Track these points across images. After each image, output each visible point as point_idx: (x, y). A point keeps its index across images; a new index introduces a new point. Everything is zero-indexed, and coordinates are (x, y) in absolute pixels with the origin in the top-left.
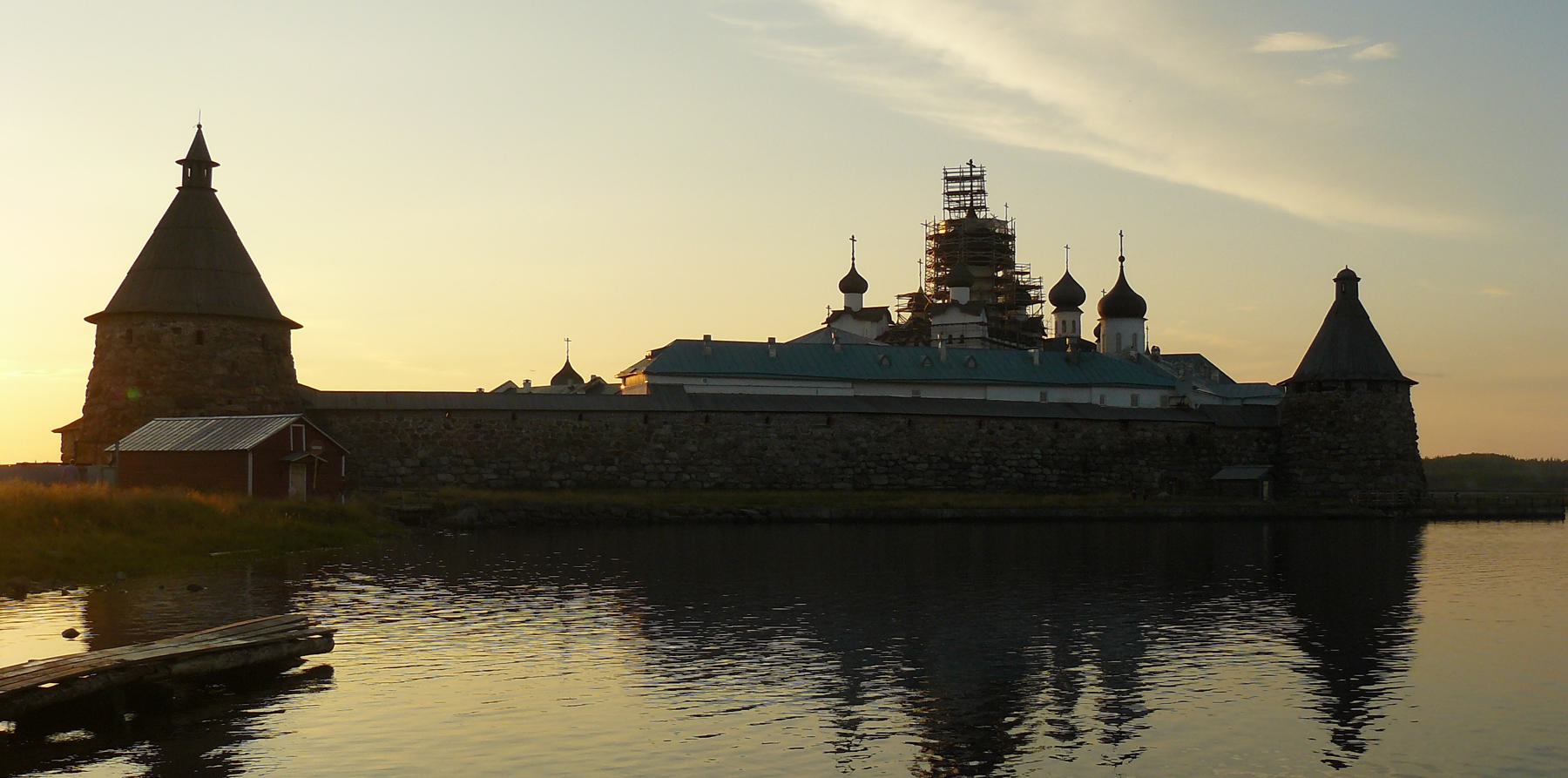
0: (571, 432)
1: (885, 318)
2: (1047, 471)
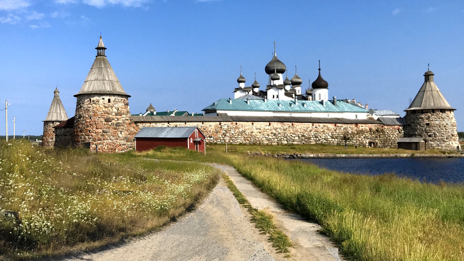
0: (201, 128)
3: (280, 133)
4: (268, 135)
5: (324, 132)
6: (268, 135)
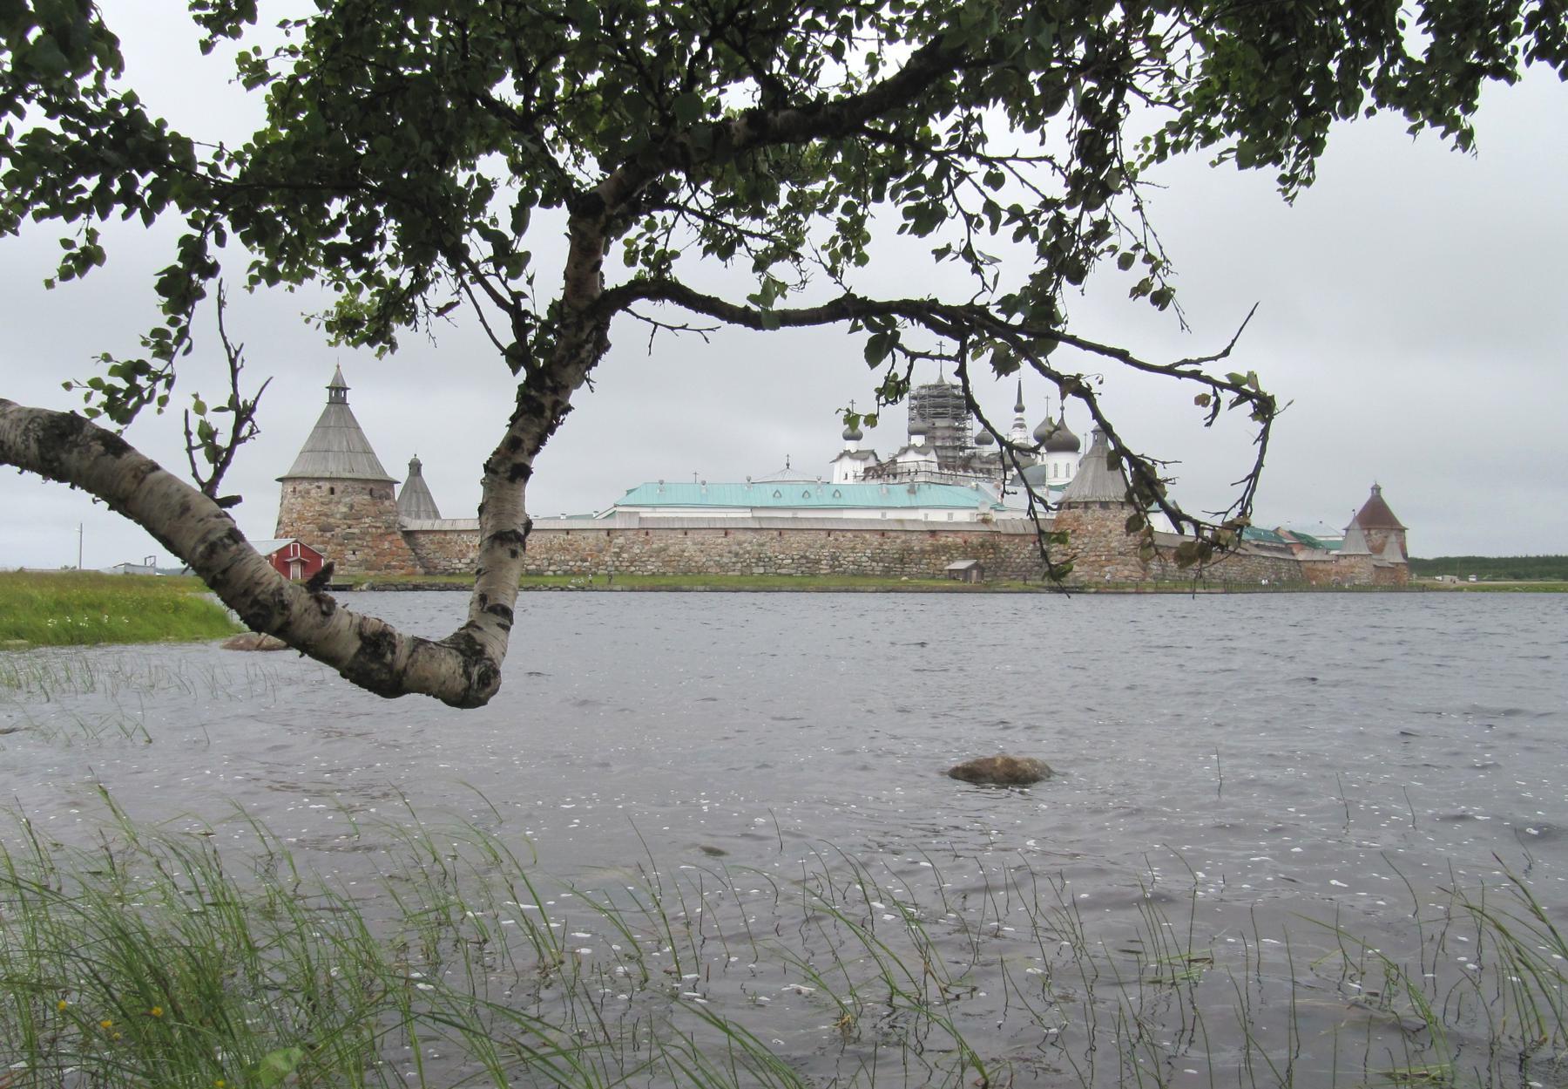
1: (872, 459)
2: (874, 564)
3: (749, 552)
4: (721, 556)
5: (853, 548)
6: (721, 556)
